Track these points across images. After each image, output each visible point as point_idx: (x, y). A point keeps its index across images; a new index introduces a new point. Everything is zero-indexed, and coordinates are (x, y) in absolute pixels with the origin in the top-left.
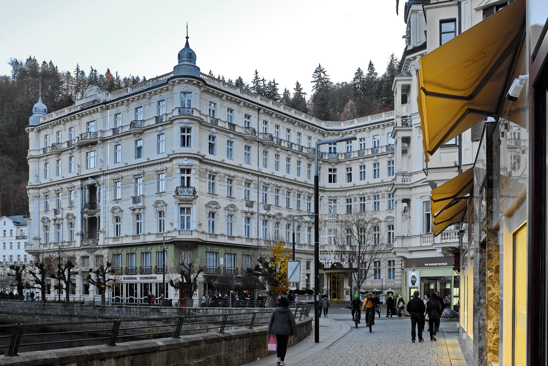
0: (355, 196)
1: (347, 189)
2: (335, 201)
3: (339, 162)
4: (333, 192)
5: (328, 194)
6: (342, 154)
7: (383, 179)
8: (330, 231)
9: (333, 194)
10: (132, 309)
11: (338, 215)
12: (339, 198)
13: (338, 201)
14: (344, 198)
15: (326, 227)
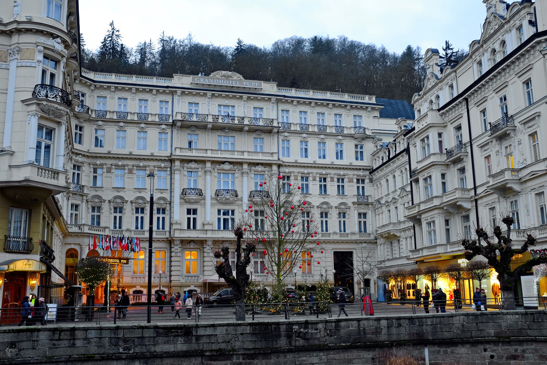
0: (109, 166)
1: (98, 155)
2: (79, 168)
3: (90, 120)
4: (80, 156)
5: (74, 157)
6: (92, 111)
7: (153, 151)
8: (72, 205)
9: (80, 159)
10: (79, 334)
11: (83, 186)
12: (85, 164)
13: (84, 168)
14: (91, 166)
15: (70, 200)
